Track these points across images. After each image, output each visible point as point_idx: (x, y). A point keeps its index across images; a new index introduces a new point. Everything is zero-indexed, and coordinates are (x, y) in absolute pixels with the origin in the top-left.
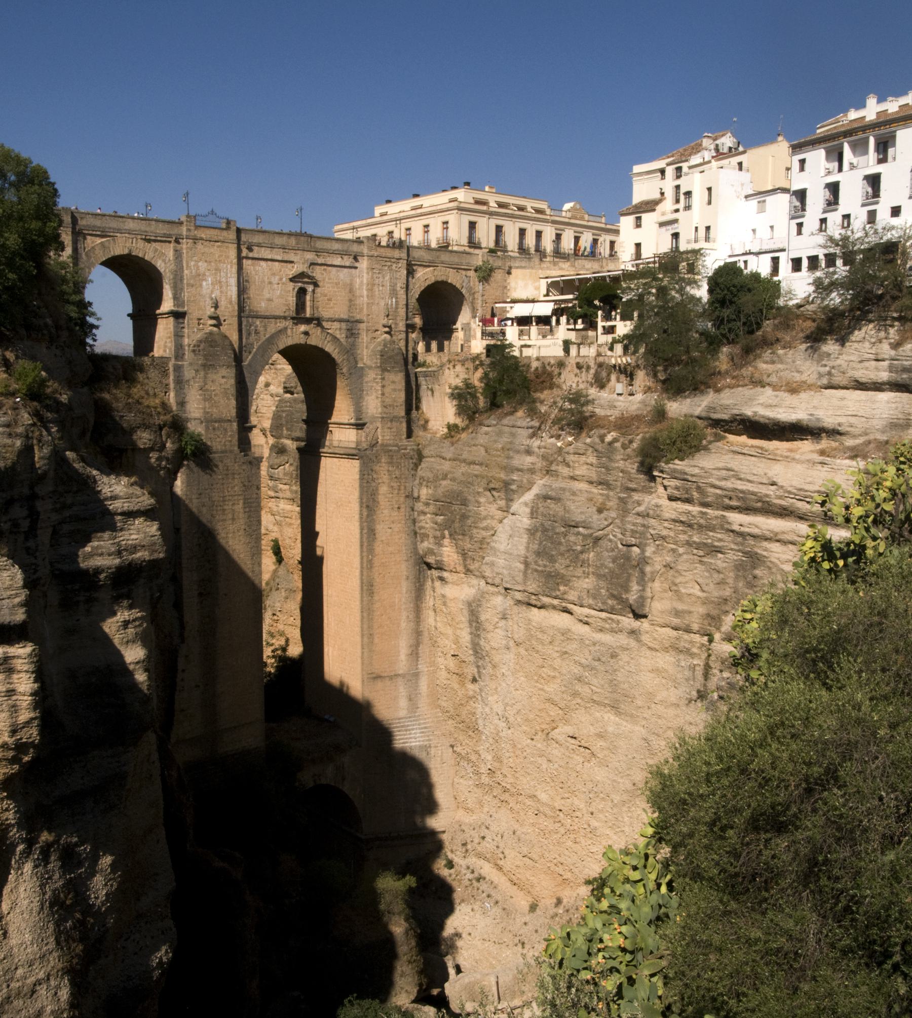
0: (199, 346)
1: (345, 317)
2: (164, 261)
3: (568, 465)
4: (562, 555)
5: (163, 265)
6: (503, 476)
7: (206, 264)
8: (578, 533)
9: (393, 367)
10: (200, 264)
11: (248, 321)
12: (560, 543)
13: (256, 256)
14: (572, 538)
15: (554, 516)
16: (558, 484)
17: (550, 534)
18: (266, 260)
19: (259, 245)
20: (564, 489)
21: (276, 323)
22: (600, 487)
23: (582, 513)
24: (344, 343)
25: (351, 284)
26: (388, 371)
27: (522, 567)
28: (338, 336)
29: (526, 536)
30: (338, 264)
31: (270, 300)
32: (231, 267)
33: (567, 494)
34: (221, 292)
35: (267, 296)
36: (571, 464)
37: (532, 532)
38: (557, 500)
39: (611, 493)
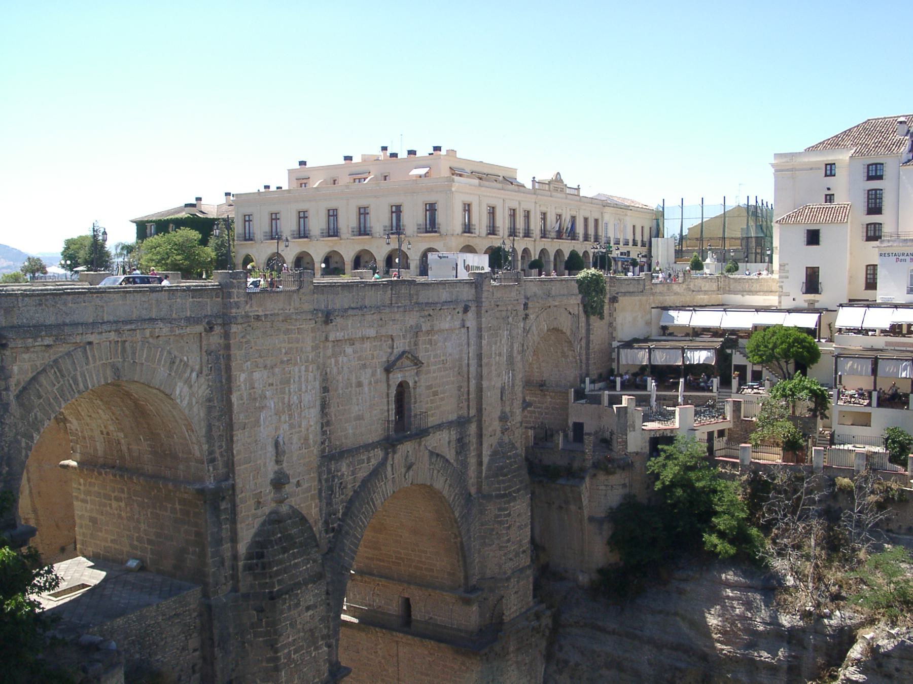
0: (261, 556)
1: (453, 417)
2: (188, 381)
5: (186, 389)
7: (265, 373)
9: (518, 490)
10: (256, 375)
11: (329, 471)
13: (340, 335)
18: (352, 342)
19: (344, 312)
21: (369, 459)
24: (455, 464)
25: (461, 359)
26: (514, 499)
28: (448, 457)
30: (447, 326)
31: (360, 418)
32: (307, 370)
34: (292, 426)
35: (355, 410)
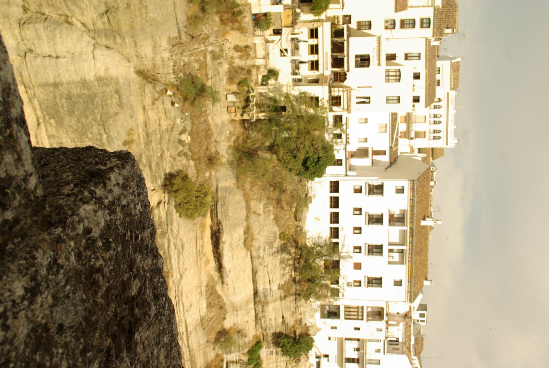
3: (153, 104)
4: (79, 121)
6: (125, 28)
8: (101, 135)
12: (87, 117)
14: (95, 130)
15: (106, 105)
16: (134, 100)
17: (91, 106)
20: (132, 108)
22: (144, 134)
23: (118, 133)
27: (51, 81)
29: (79, 78)
33: (129, 111)
36: (155, 107)
37: (84, 83)
38: (120, 105)
39: (143, 146)
